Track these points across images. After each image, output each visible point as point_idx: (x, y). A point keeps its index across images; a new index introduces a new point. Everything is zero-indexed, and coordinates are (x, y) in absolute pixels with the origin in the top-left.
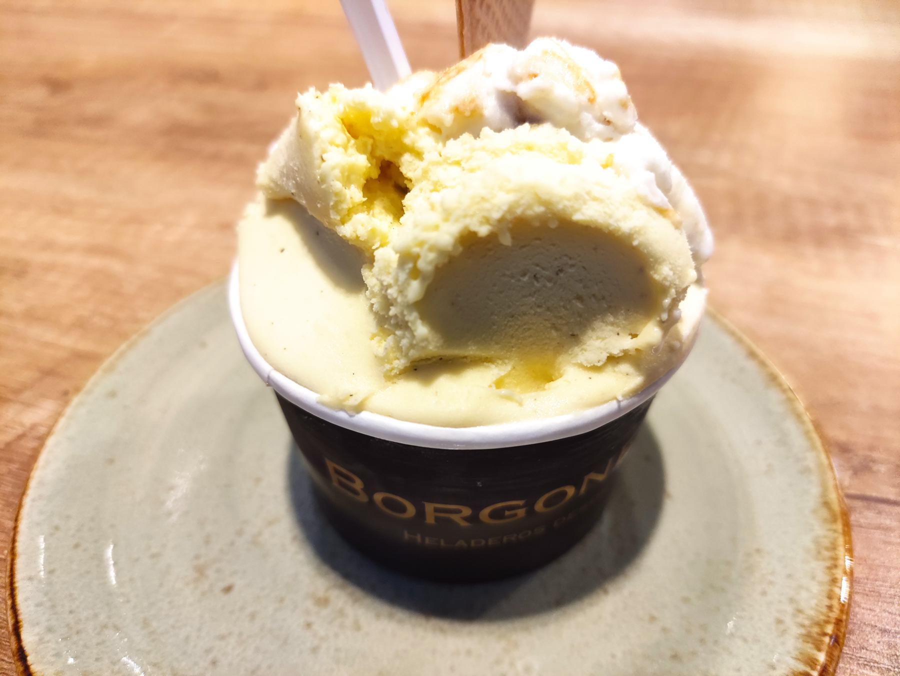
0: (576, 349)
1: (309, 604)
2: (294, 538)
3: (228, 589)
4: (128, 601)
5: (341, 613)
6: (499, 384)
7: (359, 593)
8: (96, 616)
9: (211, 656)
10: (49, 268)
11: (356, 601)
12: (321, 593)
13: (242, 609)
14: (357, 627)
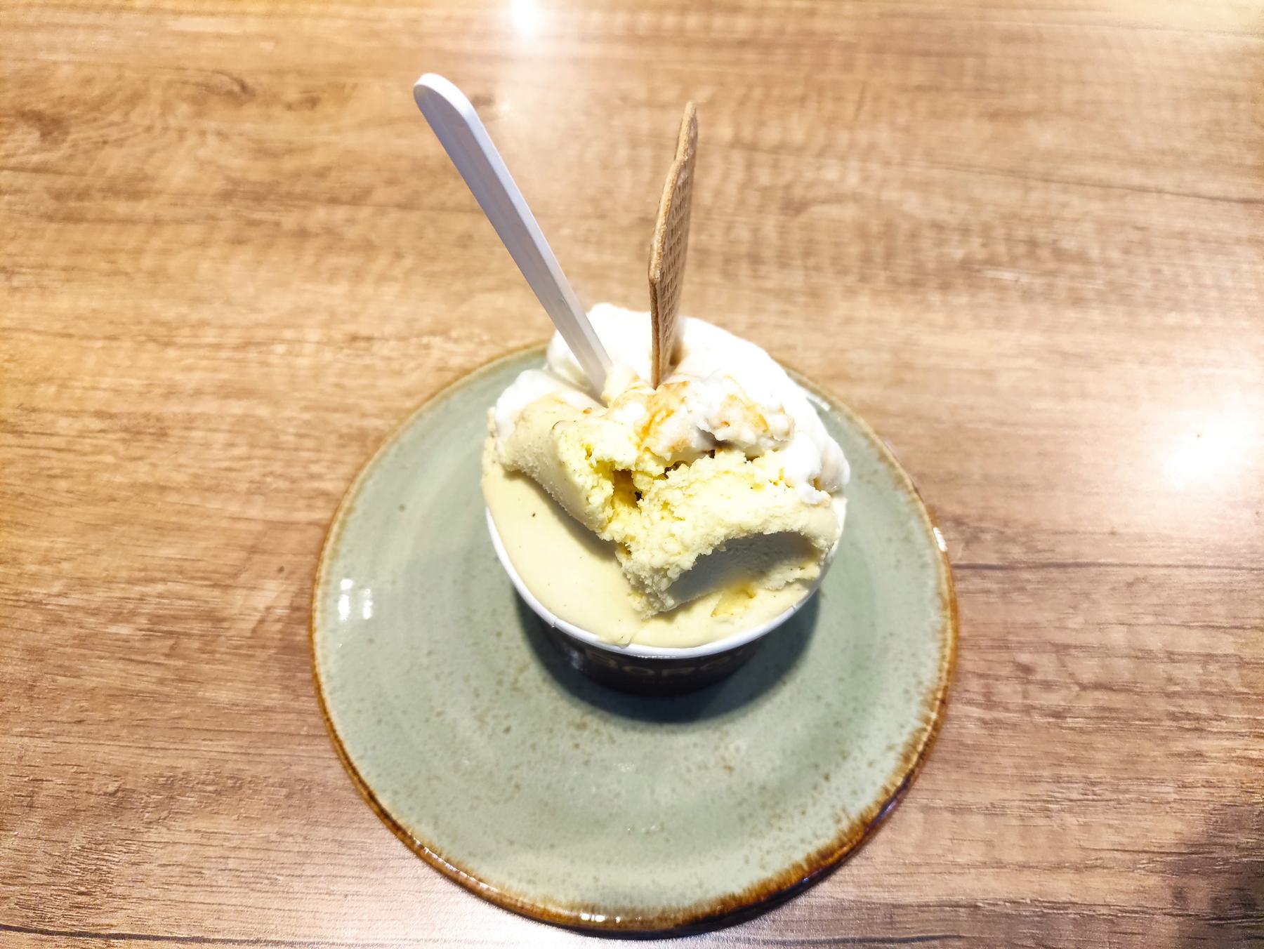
0: (765, 580)
1: (572, 730)
2: (544, 680)
3: (508, 730)
4: (436, 755)
5: (597, 732)
6: (714, 613)
7: (606, 715)
8: (419, 772)
9: (513, 782)
10: (189, 423)
11: (606, 721)
12: (578, 720)
13: (523, 743)
14: (613, 741)
